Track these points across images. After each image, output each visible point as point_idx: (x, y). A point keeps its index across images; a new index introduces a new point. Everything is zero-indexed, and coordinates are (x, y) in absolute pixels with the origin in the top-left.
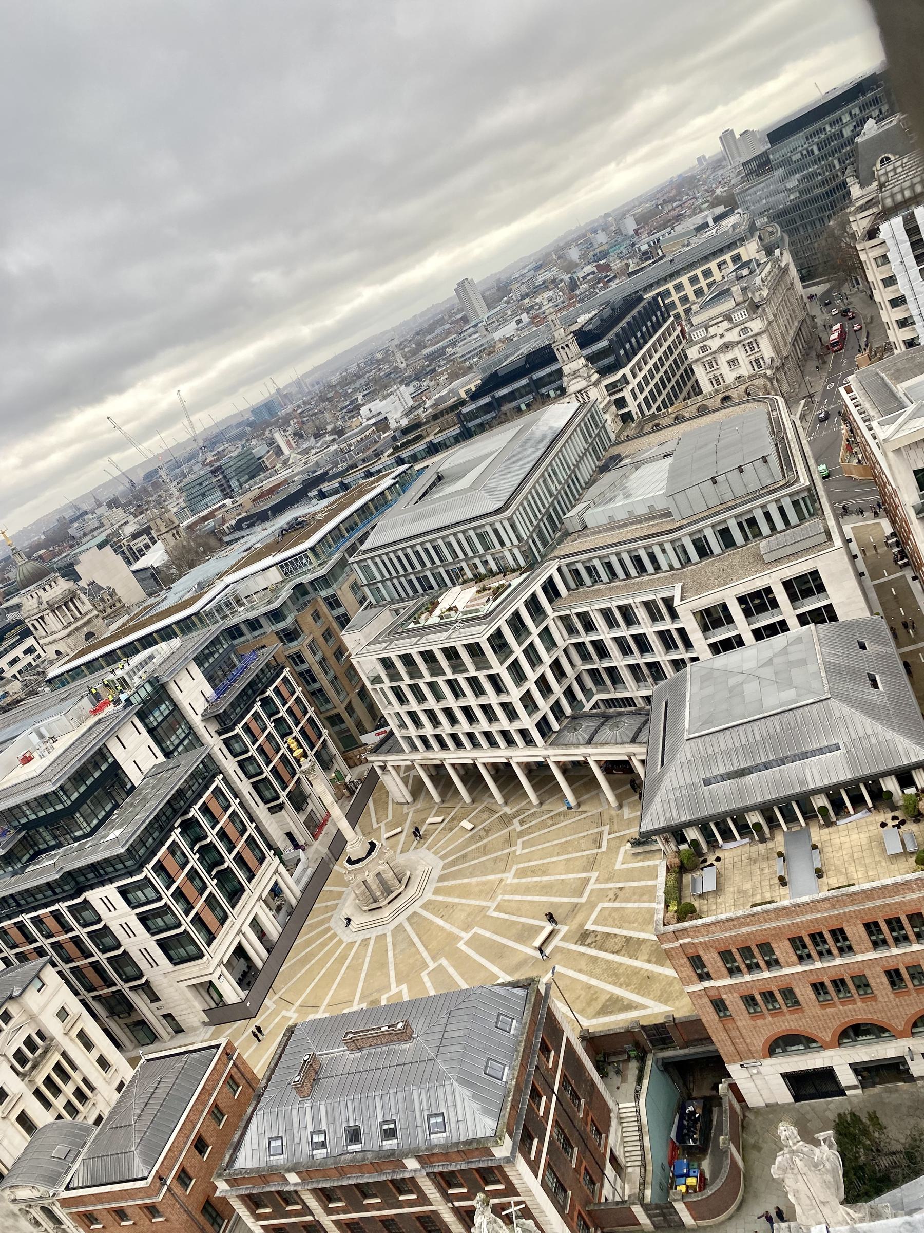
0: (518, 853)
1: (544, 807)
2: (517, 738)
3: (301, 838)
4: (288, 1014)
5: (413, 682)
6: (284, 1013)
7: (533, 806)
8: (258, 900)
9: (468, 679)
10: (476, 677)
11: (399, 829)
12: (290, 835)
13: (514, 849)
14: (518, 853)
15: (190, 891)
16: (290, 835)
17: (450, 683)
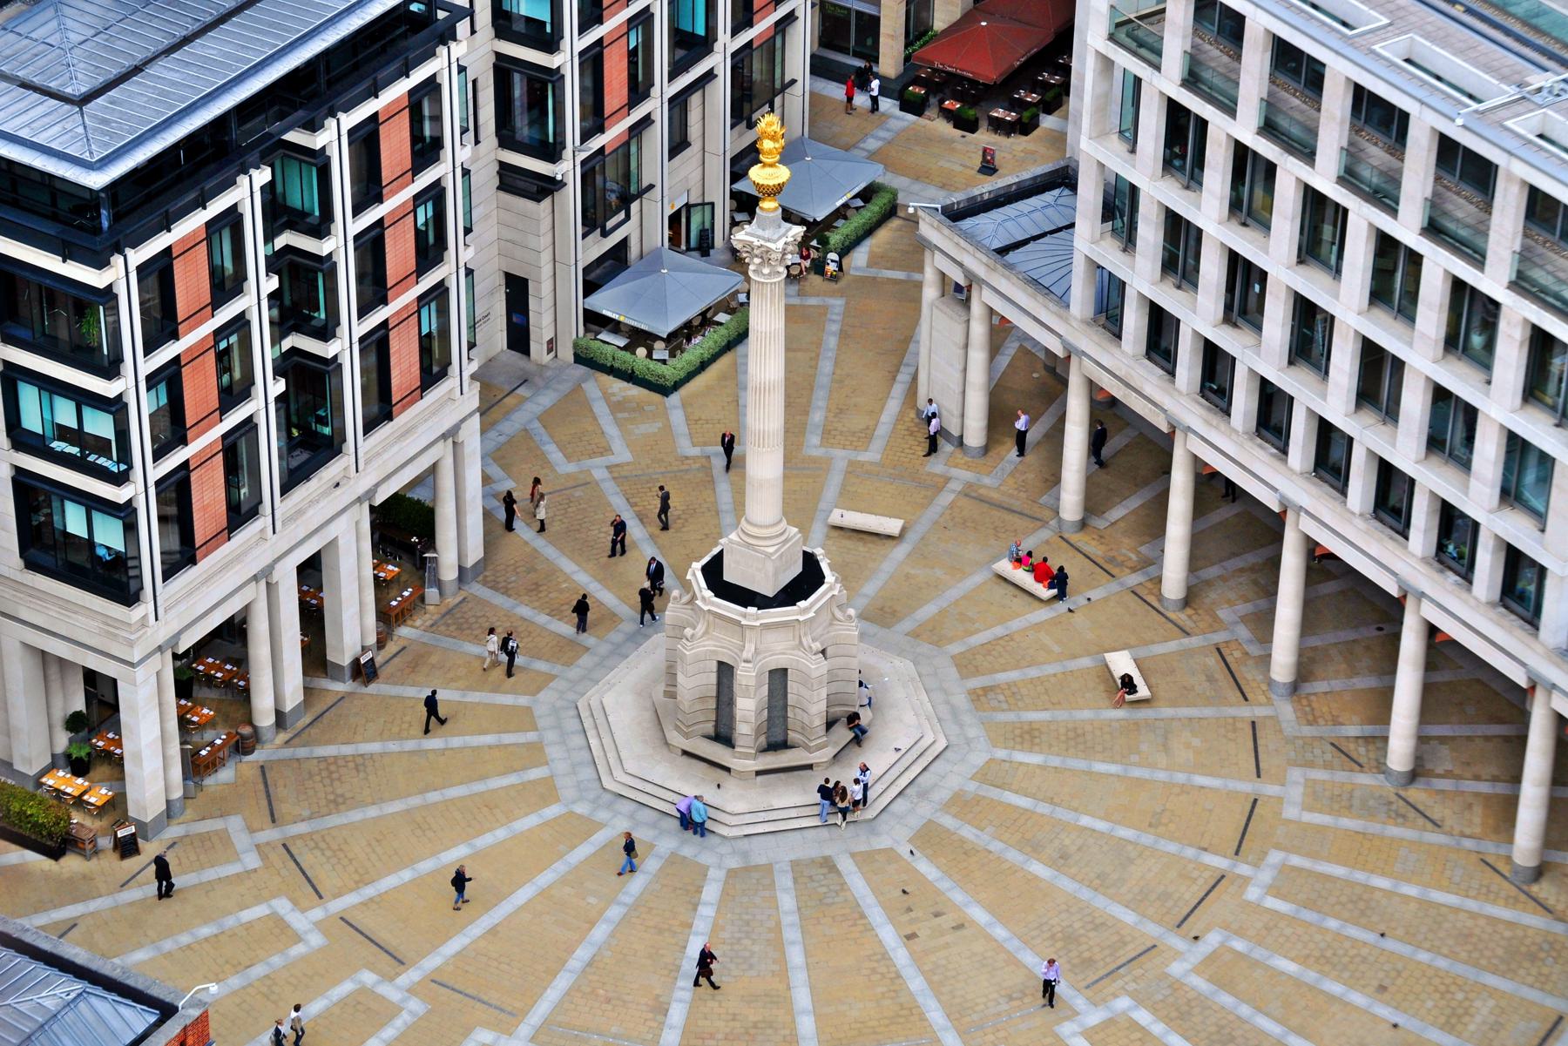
0: (1253, 893)
1: (1415, 793)
2: (1487, 565)
3: (547, 319)
4: (298, 921)
5: (1267, 149)
6: (282, 906)
7: (1381, 767)
8: (359, 500)
9: (1459, 287)
10: (1492, 308)
11: (892, 526)
12: (517, 290)
13: (1244, 869)
14: (1253, 893)
15: (200, 389)
16: (517, 290)
17: (1386, 245)
